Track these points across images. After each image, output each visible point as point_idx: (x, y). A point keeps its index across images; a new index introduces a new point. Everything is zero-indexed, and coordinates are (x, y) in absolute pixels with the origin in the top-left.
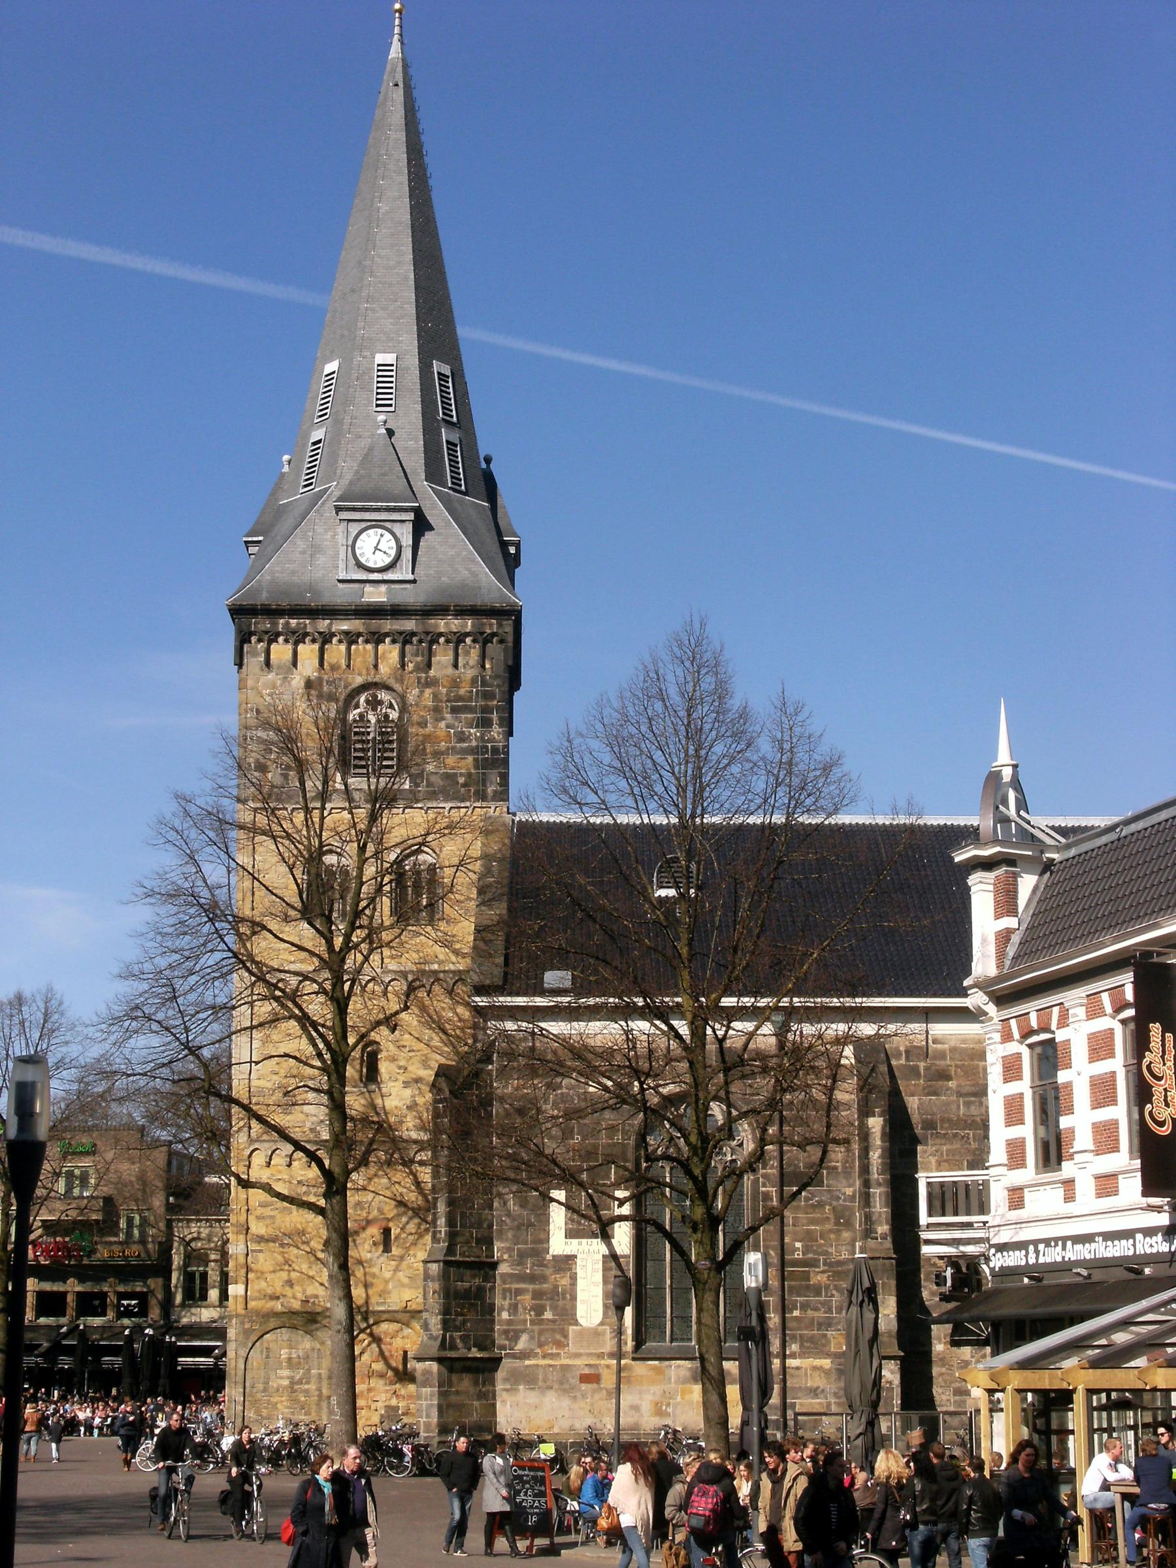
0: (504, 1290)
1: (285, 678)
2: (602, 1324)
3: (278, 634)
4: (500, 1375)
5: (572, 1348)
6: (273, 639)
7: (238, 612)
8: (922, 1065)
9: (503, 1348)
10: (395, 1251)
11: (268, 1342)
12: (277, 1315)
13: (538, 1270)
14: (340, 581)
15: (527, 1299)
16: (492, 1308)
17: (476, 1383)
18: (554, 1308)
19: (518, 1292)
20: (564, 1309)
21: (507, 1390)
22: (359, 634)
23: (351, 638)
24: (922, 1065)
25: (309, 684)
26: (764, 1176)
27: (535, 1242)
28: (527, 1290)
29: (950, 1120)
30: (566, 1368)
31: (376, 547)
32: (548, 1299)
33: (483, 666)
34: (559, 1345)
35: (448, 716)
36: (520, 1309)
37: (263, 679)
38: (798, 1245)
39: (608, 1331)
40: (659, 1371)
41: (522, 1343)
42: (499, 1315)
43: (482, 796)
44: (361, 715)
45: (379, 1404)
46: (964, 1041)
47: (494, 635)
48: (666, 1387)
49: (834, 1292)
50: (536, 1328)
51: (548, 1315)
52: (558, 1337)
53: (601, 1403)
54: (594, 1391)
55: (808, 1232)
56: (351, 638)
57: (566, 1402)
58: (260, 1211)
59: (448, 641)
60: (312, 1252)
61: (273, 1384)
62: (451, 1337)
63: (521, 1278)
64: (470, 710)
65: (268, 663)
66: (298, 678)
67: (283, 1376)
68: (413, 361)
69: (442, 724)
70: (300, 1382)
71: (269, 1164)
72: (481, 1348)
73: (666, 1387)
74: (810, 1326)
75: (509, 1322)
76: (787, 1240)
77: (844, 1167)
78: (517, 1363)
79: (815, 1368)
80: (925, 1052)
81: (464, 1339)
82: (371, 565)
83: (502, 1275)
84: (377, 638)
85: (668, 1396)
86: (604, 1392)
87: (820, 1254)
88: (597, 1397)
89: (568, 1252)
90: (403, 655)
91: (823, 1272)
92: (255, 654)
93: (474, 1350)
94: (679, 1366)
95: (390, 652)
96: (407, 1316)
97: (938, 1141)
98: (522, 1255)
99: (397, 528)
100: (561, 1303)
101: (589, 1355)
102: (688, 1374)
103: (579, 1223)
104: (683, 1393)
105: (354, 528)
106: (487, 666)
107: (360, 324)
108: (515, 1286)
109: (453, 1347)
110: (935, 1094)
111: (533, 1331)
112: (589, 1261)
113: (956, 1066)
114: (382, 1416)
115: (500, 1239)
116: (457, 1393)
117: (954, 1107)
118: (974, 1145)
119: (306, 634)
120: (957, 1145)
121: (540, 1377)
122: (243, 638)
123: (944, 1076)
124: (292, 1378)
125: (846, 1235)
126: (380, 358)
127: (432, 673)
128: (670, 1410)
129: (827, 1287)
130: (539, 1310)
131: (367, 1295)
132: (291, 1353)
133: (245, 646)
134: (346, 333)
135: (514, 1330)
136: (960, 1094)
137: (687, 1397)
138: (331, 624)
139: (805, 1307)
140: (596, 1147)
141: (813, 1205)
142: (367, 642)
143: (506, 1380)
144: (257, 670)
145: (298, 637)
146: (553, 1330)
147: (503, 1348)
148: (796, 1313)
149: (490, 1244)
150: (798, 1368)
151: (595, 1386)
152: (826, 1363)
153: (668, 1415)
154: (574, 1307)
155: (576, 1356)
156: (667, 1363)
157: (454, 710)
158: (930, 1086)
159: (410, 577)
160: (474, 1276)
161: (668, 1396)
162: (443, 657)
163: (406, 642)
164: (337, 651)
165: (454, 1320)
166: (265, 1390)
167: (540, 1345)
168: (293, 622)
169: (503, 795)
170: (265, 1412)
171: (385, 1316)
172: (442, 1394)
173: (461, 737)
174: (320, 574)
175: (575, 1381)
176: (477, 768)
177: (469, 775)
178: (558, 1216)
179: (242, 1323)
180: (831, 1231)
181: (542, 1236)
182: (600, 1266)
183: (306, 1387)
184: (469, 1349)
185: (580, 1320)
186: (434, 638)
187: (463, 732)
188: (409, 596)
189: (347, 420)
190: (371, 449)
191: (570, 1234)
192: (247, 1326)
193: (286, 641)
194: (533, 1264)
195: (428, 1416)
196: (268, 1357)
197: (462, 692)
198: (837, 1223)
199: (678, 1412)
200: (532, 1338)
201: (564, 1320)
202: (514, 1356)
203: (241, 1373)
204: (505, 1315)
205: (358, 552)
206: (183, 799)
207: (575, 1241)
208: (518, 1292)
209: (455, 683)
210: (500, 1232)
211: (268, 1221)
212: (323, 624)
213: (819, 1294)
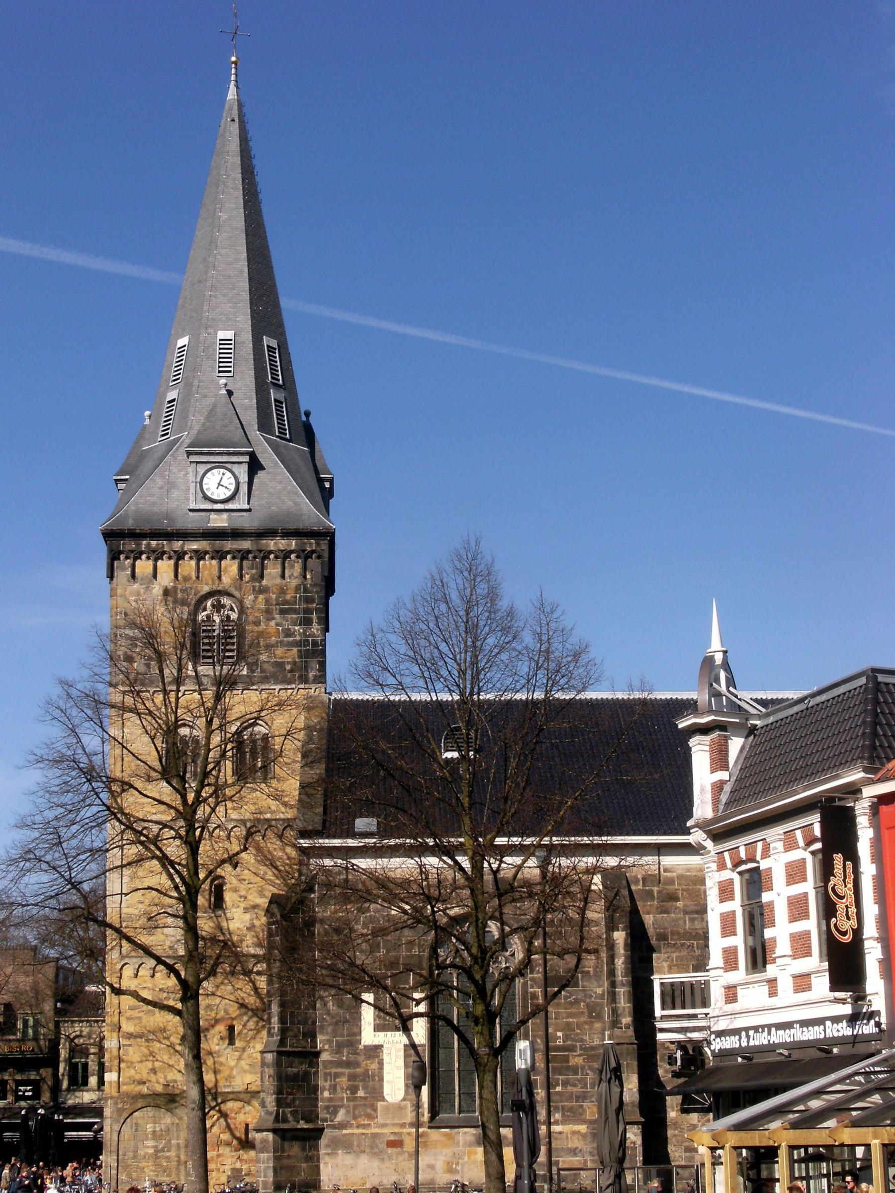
0: (326, 1074)
1: (148, 587)
2: (404, 1099)
3: (141, 553)
4: (323, 1142)
5: (380, 1120)
6: (138, 557)
7: (110, 535)
8: (656, 889)
9: (325, 1120)
10: (238, 1044)
11: (137, 1118)
12: (144, 1096)
13: (352, 1058)
14: (191, 510)
15: (343, 1081)
16: (315, 1089)
17: (304, 1149)
18: (365, 1088)
19: (337, 1075)
20: (374, 1088)
21: (329, 1154)
22: (206, 552)
23: (199, 556)
24: (656, 889)
25: (166, 592)
26: (532, 979)
27: (348, 1035)
28: (342, 1074)
29: (678, 933)
30: (375, 1136)
31: (219, 483)
32: (361, 1081)
33: (305, 577)
34: (370, 1117)
35: (277, 616)
37: (129, 589)
38: (559, 1034)
40: (450, 1137)
41: (341, 1116)
42: (322, 1093)
43: (304, 680)
44: (208, 617)
45: (226, 1167)
46: (688, 870)
47: (313, 552)
48: (456, 1150)
49: (588, 1071)
50: (351, 1103)
51: (361, 1093)
52: (369, 1111)
53: (403, 1163)
54: (398, 1154)
55: (568, 1023)
56: (199, 556)
57: (376, 1163)
58: (129, 1013)
59: (276, 557)
60: (172, 1046)
61: (141, 1152)
62: (283, 1112)
63: (339, 1064)
64: (295, 611)
65: (133, 576)
66: (157, 587)
67: (148, 1147)
68: (247, 337)
69: (273, 623)
70: (163, 1150)
71: (136, 976)
72: (308, 1121)
73: (456, 1150)
74: (570, 1098)
75: (330, 1100)
76: (550, 1030)
77: (595, 972)
78: (336, 1132)
79: (574, 1133)
80: (657, 879)
81: (293, 1113)
82: (215, 497)
83: (324, 1062)
84: (220, 555)
85: (457, 1157)
86: (406, 1154)
87: (576, 1041)
88: (400, 1158)
89: (376, 1042)
90: (241, 568)
91: (579, 1055)
92: (124, 569)
93: (302, 1122)
94: (466, 1133)
95: (231, 566)
96: (249, 1096)
97: (668, 950)
98: (340, 1046)
99: (235, 468)
100: (371, 1083)
101: (394, 1125)
102: (473, 1139)
103: (385, 1019)
104: (469, 1154)
105: (202, 469)
106: (308, 577)
107: (205, 308)
108: (334, 1070)
109: (285, 1120)
110: (666, 912)
112: (393, 1050)
113: (683, 890)
114: (229, 1177)
115: (322, 1033)
116: (289, 1157)
117: (681, 922)
118: (698, 952)
119: (164, 553)
120: (684, 953)
121: (355, 1143)
122: (114, 556)
123: (673, 898)
124: (156, 1147)
125: (598, 1025)
126: (221, 335)
127: (264, 582)
128: (459, 1168)
129: (583, 1068)
130: (354, 1090)
131: (216, 1080)
132: (155, 1127)
133: (116, 562)
134: (194, 315)
136: (686, 912)
137: (472, 1157)
138: (183, 545)
139: (565, 1084)
140: (397, 958)
141: (570, 1002)
142: (212, 558)
143: (328, 1146)
144: (125, 581)
145: (158, 555)
146: (365, 1105)
147: (325, 1120)
148: (559, 1089)
149: (314, 1037)
150: (560, 1133)
151: (399, 1149)
152: (583, 1128)
153: (457, 1172)
154: (382, 1087)
155: (384, 1126)
156: (456, 1130)
157: (283, 612)
158: (663, 906)
159: (246, 507)
160: (301, 1063)
161: (457, 1157)
162: (272, 570)
163: (243, 558)
164: (188, 566)
165: (286, 1098)
166: (135, 1157)
167: (355, 1118)
168: (154, 543)
169: (321, 678)
170: (134, 1175)
171: (231, 1096)
172: (276, 1158)
173: (288, 633)
174: (174, 505)
175: (383, 1146)
176: (300, 657)
177: (294, 663)
178: (368, 1014)
179: (116, 1103)
180: (585, 1023)
181: (356, 1030)
182: (402, 1053)
183: (168, 1154)
184: (298, 1122)
185: (386, 1097)
186: (265, 555)
187: (289, 629)
188: (245, 522)
189: (196, 383)
190: (215, 406)
191: (378, 1028)
192: (120, 1106)
193: (148, 558)
194: (349, 1053)
195: (265, 1176)
196: (136, 1130)
197: (288, 597)
198: (590, 1016)
199: (466, 1169)
200: (348, 1112)
201: (373, 1097)
202: (334, 1127)
203: (115, 1143)
204: (326, 1094)
205: (205, 487)
206: (66, 684)
207: (382, 1034)
208: (337, 1075)
209: (282, 591)
210: (322, 1027)
211: (137, 1021)
212: (177, 545)
213: (576, 1073)
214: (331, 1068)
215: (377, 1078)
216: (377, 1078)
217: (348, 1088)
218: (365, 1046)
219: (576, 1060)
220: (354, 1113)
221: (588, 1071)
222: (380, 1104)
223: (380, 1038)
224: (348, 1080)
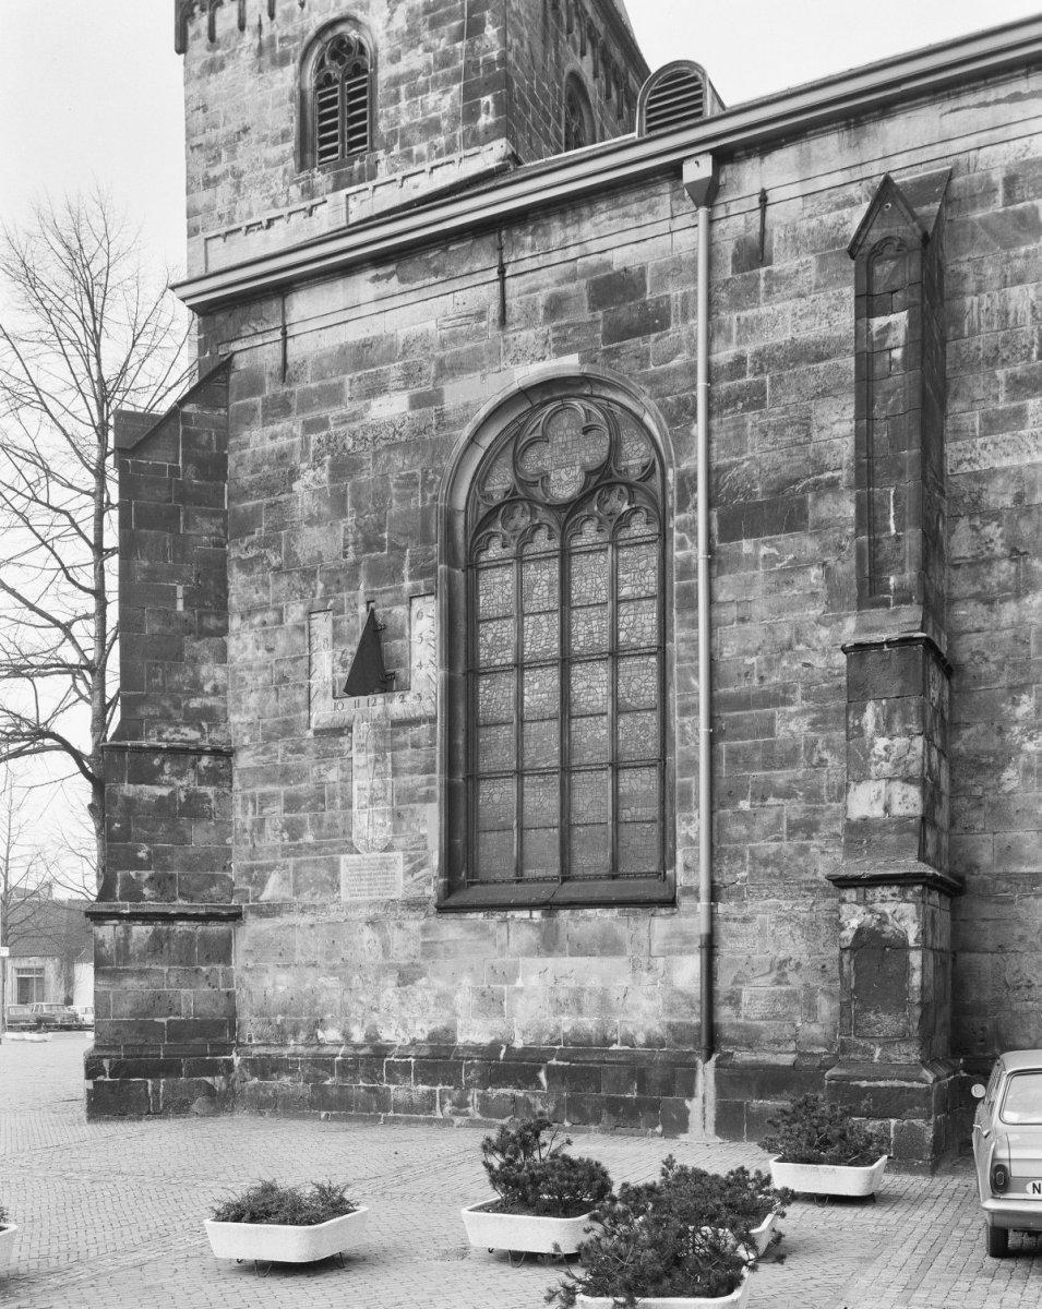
13: (293, 761)
19: (266, 799)
20: (332, 826)
49: (826, 755)
50: (291, 861)
51: (309, 838)
91: (804, 712)
100: (327, 814)
108: (260, 789)
130: (294, 830)
154: (348, 820)
160: (180, 774)
208: (266, 799)
210: (238, 699)
214: (254, 786)
215: (338, 801)
216: (338, 801)
218: (316, 732)
219: (793, 726)
221: (826, 755)
222: (344, 858)
223: (350, 707)
224: (285, 811)
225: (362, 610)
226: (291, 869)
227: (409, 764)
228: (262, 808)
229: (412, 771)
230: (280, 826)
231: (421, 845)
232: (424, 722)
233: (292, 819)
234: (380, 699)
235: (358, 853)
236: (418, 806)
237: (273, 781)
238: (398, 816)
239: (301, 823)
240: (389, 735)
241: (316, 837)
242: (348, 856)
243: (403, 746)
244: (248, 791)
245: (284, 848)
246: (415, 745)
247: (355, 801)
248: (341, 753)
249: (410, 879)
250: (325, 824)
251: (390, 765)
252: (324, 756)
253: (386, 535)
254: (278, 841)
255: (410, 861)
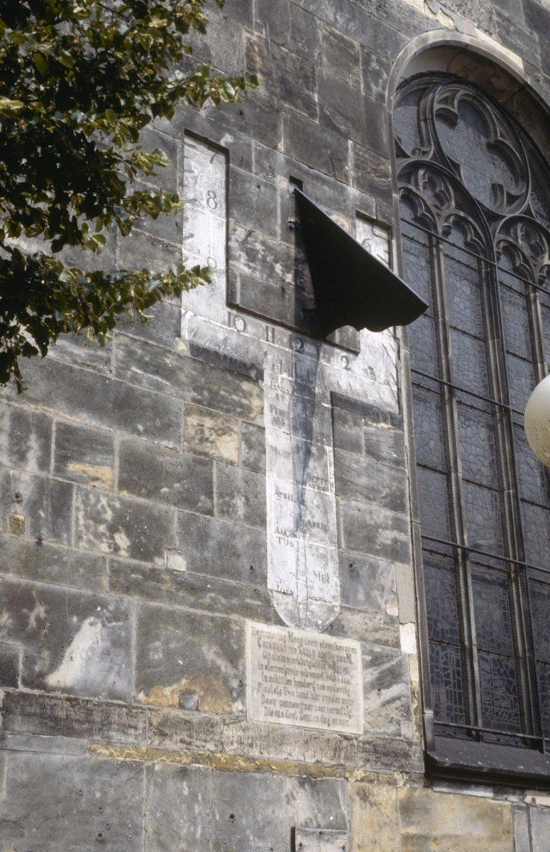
13: (144, 382)
15: (100, 478)
19: (73, 444)
20: (227, 549)
36: (78, 515)
39: (358, 659)
41: (81, 663)
50: (133, 603)
52: (210, 653)
100: (217, 523)
108: (60, 415)
111: (121, 615)
130: (147, 535)
135: (45, 597)
146: (193, 624)
200: (118, 643)
208: (73, 444)
214: (47, 400)
215: (239, 502)
216: (239, 502)
217: (126, 521)
220: (143, 655)
222: (253, 628)
224: (123, 484)
225: (283, 184)
226: (134, 620)
227: (363, 480)
228: (63, 459)
229: (370, 494)
230: (109, 515)
231: (389, 636)
232: (385, 421)
233: (139, 509)
234: (309, 348)
235: (280, 622)
236: (382, 562)
237: (97, 410)
238: (350, 570)
239: (159, 524)
240: (328, 415)
241: (192, 565)
242: (262, 627)
243: (355, 446)
244: (29, 408)
245: (117, 570)
246: (373, 452)
247: (271, 517)
248: (245, 411)
249: (376, 700)
250: (211, 543)
251: (331, 470)
252: (211, 403)
253: (316, 98)
254: (104, 547)
255: (375, 661)
